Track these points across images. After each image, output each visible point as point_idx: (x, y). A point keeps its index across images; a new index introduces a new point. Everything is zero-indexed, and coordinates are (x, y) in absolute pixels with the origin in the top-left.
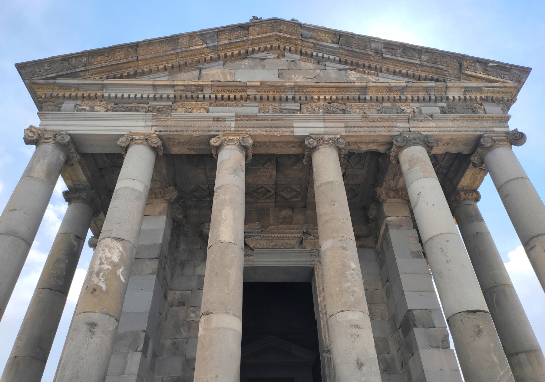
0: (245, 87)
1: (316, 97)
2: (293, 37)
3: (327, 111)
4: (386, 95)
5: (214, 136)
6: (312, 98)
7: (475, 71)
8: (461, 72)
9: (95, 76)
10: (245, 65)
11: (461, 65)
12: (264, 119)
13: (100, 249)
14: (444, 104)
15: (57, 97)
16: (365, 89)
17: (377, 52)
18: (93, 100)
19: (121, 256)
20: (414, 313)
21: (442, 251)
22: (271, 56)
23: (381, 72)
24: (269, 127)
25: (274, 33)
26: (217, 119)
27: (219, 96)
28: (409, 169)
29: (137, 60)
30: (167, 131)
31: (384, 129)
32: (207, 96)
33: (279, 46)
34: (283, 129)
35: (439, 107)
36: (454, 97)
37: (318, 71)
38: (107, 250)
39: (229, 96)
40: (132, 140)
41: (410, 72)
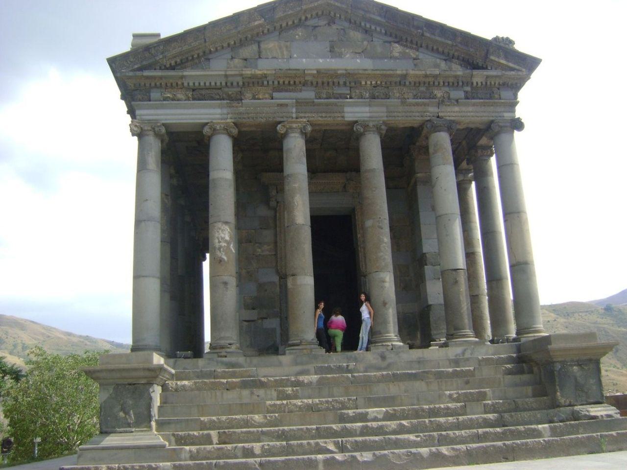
1: (363, 83)
3: (373, 97)
4: (423, 80)
5: (280, 123)
6: (361, 83)
8: (487, 55)
9: (170, 60)
10: (298, 35)
12: (319, 105)
13: (215, 230)
14: (468, 89)
16: (405, 76)
17: (418, 28)
18: (175, 87)
19: (230, 235)
20: (427, 255)
21: (445, 227)
22: (322, 22)
23: (421, 47)
24: (324, 112)
26: (281, 105)
27: (281, 82)
28: (433, 154)
29: (205, 41)
30: (240, 118)
31: (417, 114)
32: (271, 83)
33: (330, 13)
34: (336, 115)
36: (477, 83)
37: (365, 43)
38: (220, 231)
39: (289, 82)
40: (215, 130)
41: (446, 51)
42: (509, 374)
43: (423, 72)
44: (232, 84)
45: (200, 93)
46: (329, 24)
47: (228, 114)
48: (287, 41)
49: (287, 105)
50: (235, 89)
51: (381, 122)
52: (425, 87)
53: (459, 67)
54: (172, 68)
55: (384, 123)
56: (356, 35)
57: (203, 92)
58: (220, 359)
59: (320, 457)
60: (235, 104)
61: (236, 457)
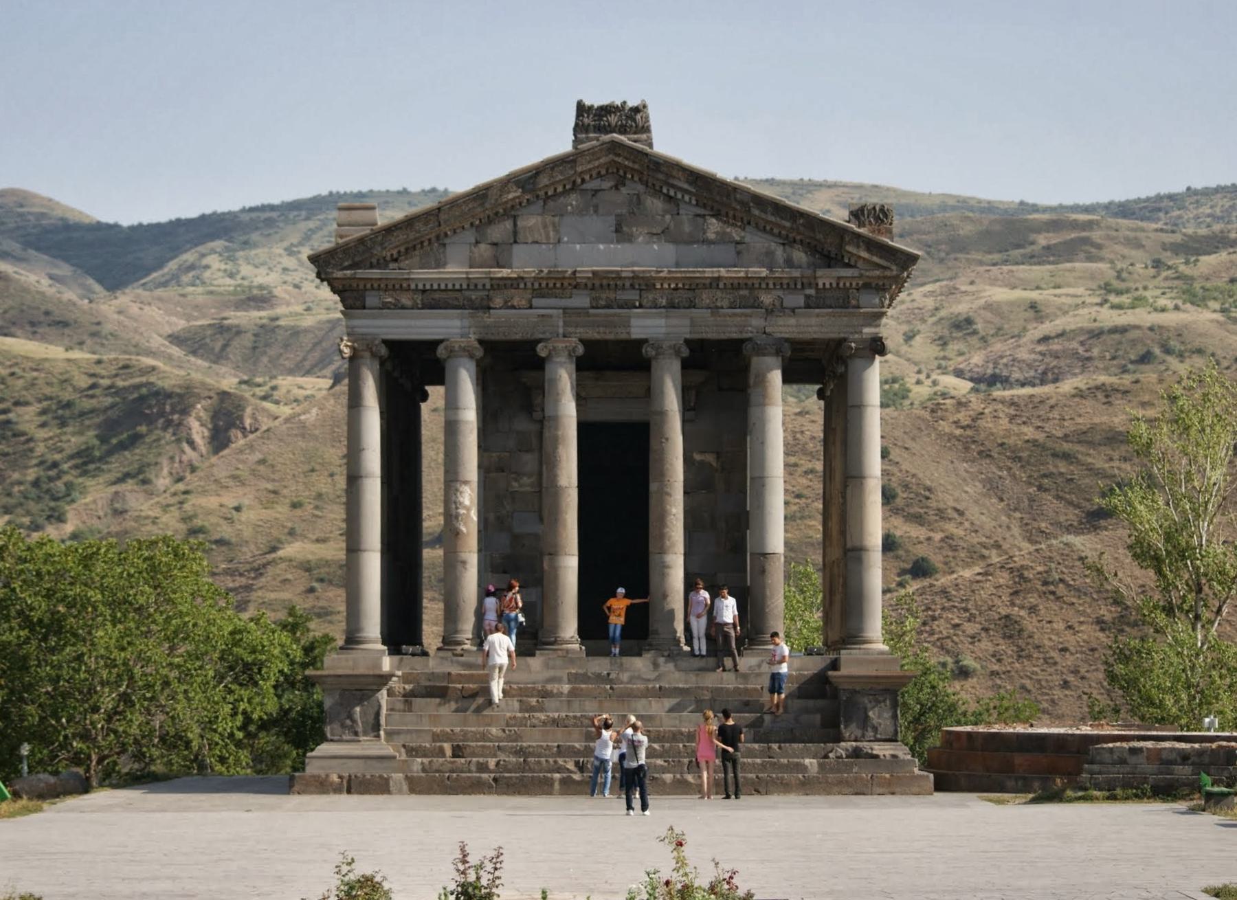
1: (658, 286)
2: (636, 166)
3: (672, 306)
5: (539, 341)
7: (858, 247)
11: (842, 238)
12: (595, 315)
14: (812, 292)
17: (741, 203)
22: (607, 184)
23: (749, 223)
25: (611, 156)
27: (544, 285)
31: (734, 329)
32: (529, 285)
34: (619, 330)
37: (668, 217)
41: (784, 232)
42: (799, 698)
44: (476, 285)
45: (434, 299)
46: (616, 187)
49: (550, 316)
52: (745, 294)
53: (803, 255)
54: (396, 260)
55: (687, 341)
56: (654, 204)
57: (437, 296)
58: (455, 658)
59: (557, 776)
60: (480, 313)
61: (470, 771)
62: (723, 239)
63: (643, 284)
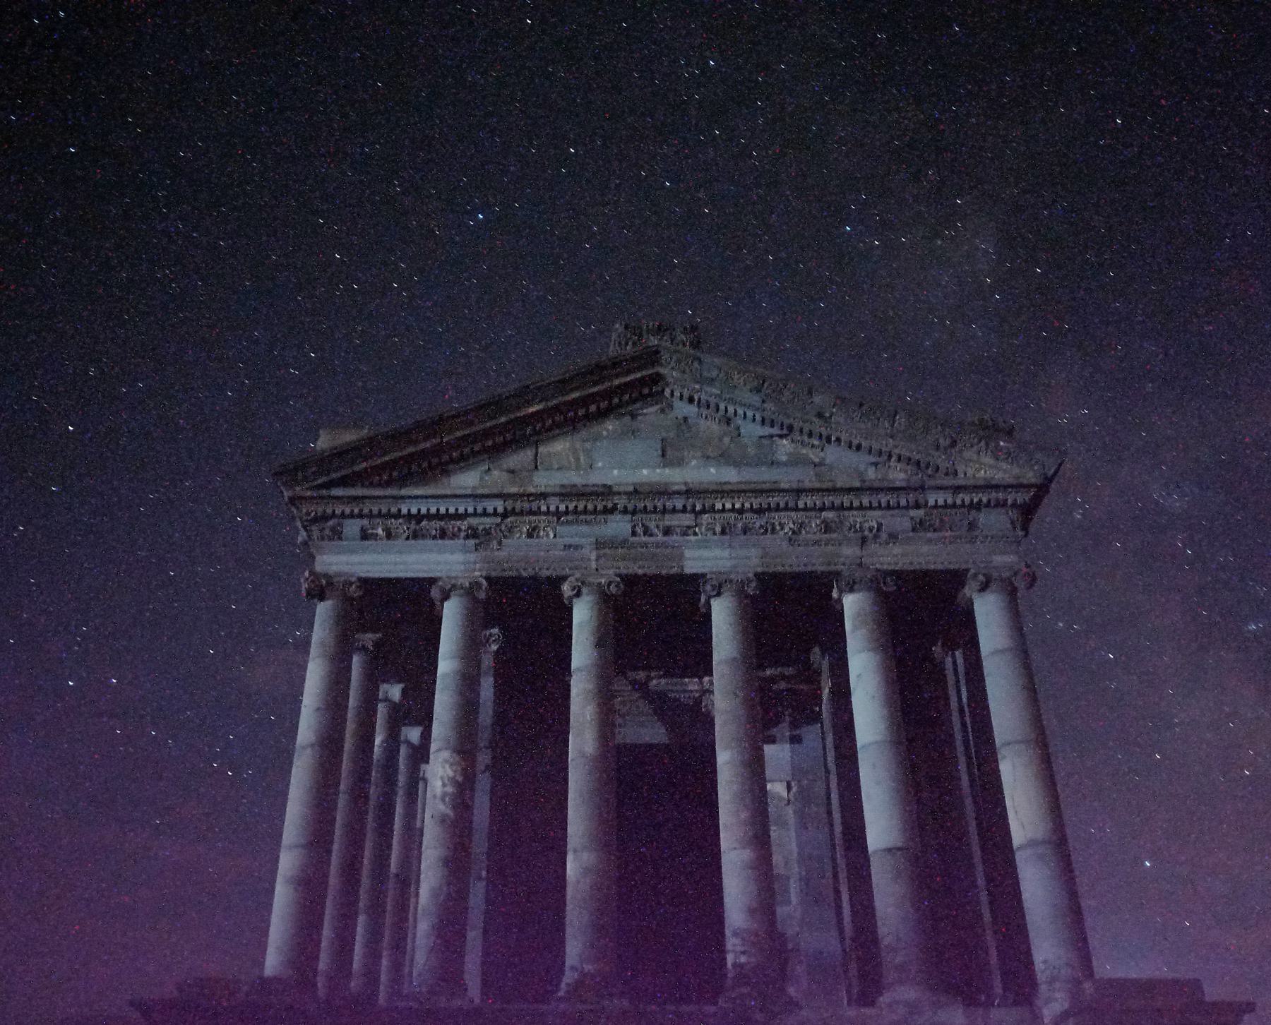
0: (607, 491)
4: (828, 500)
14: (920, 513)
15: (333, 515)
26: (567, 547)
32: (552, 508)
35: (912, 518)
37: (727, 440)
41: (876, 446)
43: (830, 485)
46: (663, 411)
47: (475, 563)
48: (587, 441)
49: (577, 547)
50: (488, 520)
51: (751, 575)
56: (709, 427)
62: (795, 461)
63: (698, 499)
